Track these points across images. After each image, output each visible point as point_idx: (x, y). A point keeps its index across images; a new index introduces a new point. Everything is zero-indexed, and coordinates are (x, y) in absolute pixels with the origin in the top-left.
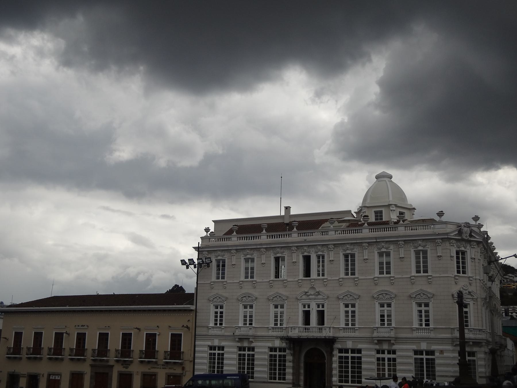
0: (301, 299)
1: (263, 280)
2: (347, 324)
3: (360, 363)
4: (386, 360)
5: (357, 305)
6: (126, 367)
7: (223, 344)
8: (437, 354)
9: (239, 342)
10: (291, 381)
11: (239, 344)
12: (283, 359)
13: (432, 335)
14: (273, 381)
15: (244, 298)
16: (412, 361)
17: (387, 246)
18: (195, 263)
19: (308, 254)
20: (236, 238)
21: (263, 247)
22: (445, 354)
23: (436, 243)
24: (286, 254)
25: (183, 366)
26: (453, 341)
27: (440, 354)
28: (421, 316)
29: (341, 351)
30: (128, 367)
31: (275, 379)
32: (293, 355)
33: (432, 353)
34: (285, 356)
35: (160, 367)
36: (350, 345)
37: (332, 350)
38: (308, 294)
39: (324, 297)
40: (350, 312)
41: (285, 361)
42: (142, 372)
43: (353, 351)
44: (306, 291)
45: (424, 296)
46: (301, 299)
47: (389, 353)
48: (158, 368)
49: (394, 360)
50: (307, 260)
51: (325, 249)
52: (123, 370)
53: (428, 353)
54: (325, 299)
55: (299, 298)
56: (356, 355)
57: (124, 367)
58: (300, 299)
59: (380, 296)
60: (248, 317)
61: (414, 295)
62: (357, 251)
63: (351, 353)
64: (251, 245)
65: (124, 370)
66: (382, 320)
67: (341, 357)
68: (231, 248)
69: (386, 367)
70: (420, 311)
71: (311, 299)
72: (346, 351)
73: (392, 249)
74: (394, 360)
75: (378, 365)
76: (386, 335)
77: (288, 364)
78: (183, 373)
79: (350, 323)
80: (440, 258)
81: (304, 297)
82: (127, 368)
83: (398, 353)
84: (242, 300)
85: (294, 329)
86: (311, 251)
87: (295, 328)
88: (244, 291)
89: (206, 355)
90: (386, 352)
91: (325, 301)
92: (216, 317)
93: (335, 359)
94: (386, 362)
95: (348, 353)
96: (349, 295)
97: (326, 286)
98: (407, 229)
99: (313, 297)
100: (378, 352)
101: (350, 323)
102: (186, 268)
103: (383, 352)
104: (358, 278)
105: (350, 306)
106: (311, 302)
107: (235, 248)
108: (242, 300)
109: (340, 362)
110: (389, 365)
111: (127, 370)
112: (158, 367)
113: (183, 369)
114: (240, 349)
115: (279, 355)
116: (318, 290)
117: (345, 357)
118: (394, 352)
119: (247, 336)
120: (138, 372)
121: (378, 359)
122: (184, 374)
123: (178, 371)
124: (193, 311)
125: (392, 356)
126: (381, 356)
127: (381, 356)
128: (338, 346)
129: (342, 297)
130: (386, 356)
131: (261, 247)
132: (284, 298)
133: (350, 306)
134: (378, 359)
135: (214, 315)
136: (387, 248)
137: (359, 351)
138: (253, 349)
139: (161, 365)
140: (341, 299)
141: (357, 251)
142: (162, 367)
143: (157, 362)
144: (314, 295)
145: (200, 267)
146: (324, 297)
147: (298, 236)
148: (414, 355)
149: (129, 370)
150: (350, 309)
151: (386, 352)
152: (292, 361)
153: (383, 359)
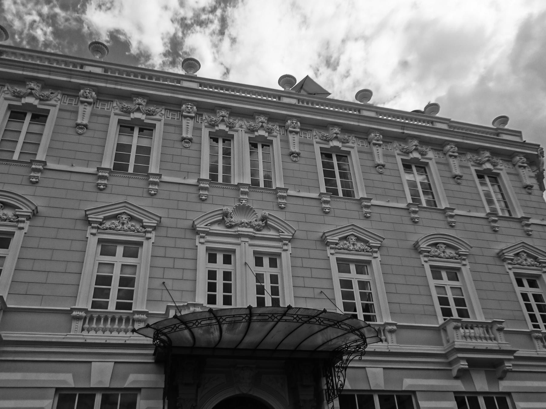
0: (208, 234)
39: (283, 232)
46: (208, 234)
71: (238, 236)
96: (354, 238)
106: (239, 244)
140: (333, 243)
144: (249, 225)
146: (283, 232)
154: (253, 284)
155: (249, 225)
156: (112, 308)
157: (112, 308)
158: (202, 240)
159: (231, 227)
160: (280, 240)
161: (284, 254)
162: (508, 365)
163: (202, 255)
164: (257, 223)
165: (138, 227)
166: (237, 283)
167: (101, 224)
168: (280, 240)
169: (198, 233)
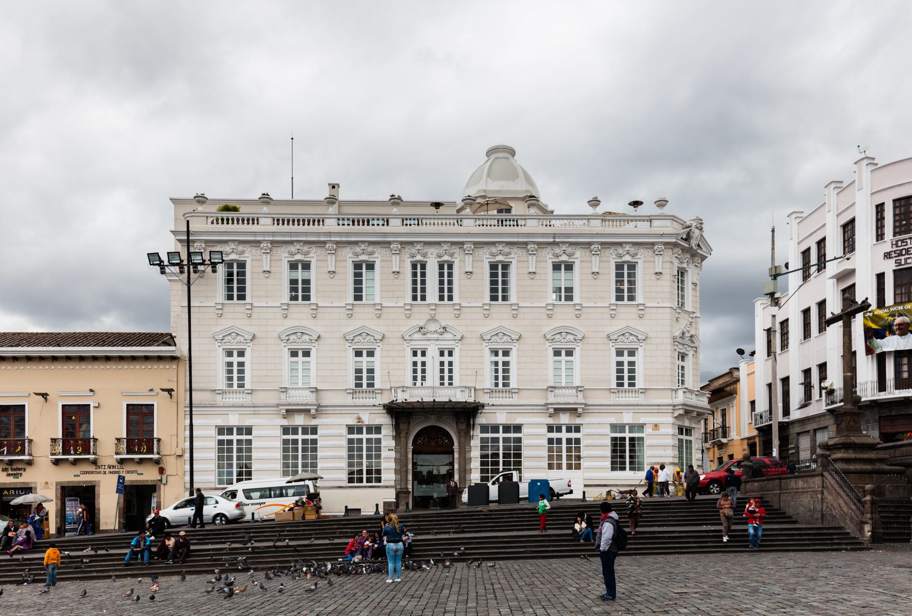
0: (411, 340)
1: (332, 303)
2: (497, 385)
3: (519, 448)
4: (564, 442)
5: (247, 353)
6: (15, 474)
7: (247, 422)
8: (648, 430)
9: (284, 418)
10: (393, 483)
11: (285, 422)
12: (375, 448)
13: (640, 399)
14: (374, 484)
15: (292, 337)
16: (608, 442)
17: (570, 250)
18: (163, 262)
19: (422, 259)
20: (270, 219)
21: (332, 239)
22: (662, 430)
23: (261, 249)
24: (379, 257)
25: (160, 466)
26: (674, 410)
27: (653, 430)
28: (496, 371)
29: (485, 429)
30: (21, 474)
31: (360, 480)
32: (397, 437)
33: (641, 427)
34: (378, 441)
35: (105, 470)
36: (501, 418)
37: (470, 426)
38: (424, 330)
40: (235, 365)
41: (379, 449)
42: (57, 484)
43: (507, 429)
44: (422, 324)
45: (631, 338)
46: (411, 340)
47: (569, 430)
48: (100, 473)
49: (578, 441)
50: (418, 269)
51: (456, 250)
52: (8, 482)
53: (632, 427)
54: (457, 340)
55: (407, 337)
56: (512, 435)
57: (9, 475)
58: (408, 340)
59: (558, 337)
60: (365, 371)
61: (616, 336)
62: (380, 258)
63: (302, 434)
64: (306, 234)
65: (11, 480)
66: (359, 378)
67: (483, 440)
68: (326, 239)
69: (564, 454)
70: (230, 364)
71: (429, 340)
72: (495, 429)
73: (577, 258)
74: (578, 441)
75: (550, 450)
76: (572, 400)
77: (384, 453)
78: (161, 480)
79: (500, 381)
80: (596, 277)
81: (418, 336)
82: (16, 476)
83: (524, 430)
84: (288, 340)
85: (403, 391)
86: (429, 253)
87: (405, 389)
88: (289, 323)
89: (214, 444)
90: (564, 428)
91: (457, 345)
92: (230, 372)
93: (475, 443)
94: (564, 445)
95: (498, 432)
96: (501, 334)
97: (578, 316)
98: (609, 224)
99: (436, 336)
100: (550, 429)
101: (500, 381)
102: (159, 272)
103: (559, 429)
104: (382, 304)
105: (626, 353)
107: (271, 239)
108: (288, 340)
109: (482, 448)
110: (569, 450)
111: (16, 480)
112: (98, 470)
113: (162, 471)
114: (286, 430)
115: (367, 439)
116: (444, 324)
117: (492, 438)
118: (577, 430)
119: (307, 404)
120: (47, 483)
121: (550, 441)
122: (164, 481)
123: (148, 475)
124: (177, 361)
125: (573, 435)
126: (555, 435)
127: (555, 435)
128: (482, 420)
129: (488, 337)
130: (564, 435)
131: (329, 239)
132: (377, 337)
133: (626, 353)
134: (550, 441)
135: (225, 368)
136: (569, 256)
137: (518, 428)
138: (314, 430)
139: (106, 467)
140: (487, 340)
141: (380, 258)
142: (107, 470)
143: (159, 460)
144: (436, 332)
145: (195, 272)
147: (272, 223)
148: (481, 433)
149: (20, 480)
150: (501, 359)
151: (564, 428)
152: (394, 448)
153: (559, 441)
154: (438, 367)
155: (436, 332)
156: (365, 386)
157: (365, 386)
158: (408, 345)
159: (424, 334)
160: (454, 340)
161: (456, 348)
162: (580, 410)
163: (409, 353)
164: (440, 331)
165: (372, 338)
166: (428, 368)
167: (353, 340)
168: (454, 340)
169: (405, 340)
